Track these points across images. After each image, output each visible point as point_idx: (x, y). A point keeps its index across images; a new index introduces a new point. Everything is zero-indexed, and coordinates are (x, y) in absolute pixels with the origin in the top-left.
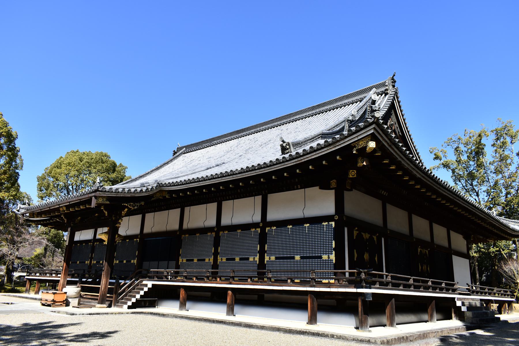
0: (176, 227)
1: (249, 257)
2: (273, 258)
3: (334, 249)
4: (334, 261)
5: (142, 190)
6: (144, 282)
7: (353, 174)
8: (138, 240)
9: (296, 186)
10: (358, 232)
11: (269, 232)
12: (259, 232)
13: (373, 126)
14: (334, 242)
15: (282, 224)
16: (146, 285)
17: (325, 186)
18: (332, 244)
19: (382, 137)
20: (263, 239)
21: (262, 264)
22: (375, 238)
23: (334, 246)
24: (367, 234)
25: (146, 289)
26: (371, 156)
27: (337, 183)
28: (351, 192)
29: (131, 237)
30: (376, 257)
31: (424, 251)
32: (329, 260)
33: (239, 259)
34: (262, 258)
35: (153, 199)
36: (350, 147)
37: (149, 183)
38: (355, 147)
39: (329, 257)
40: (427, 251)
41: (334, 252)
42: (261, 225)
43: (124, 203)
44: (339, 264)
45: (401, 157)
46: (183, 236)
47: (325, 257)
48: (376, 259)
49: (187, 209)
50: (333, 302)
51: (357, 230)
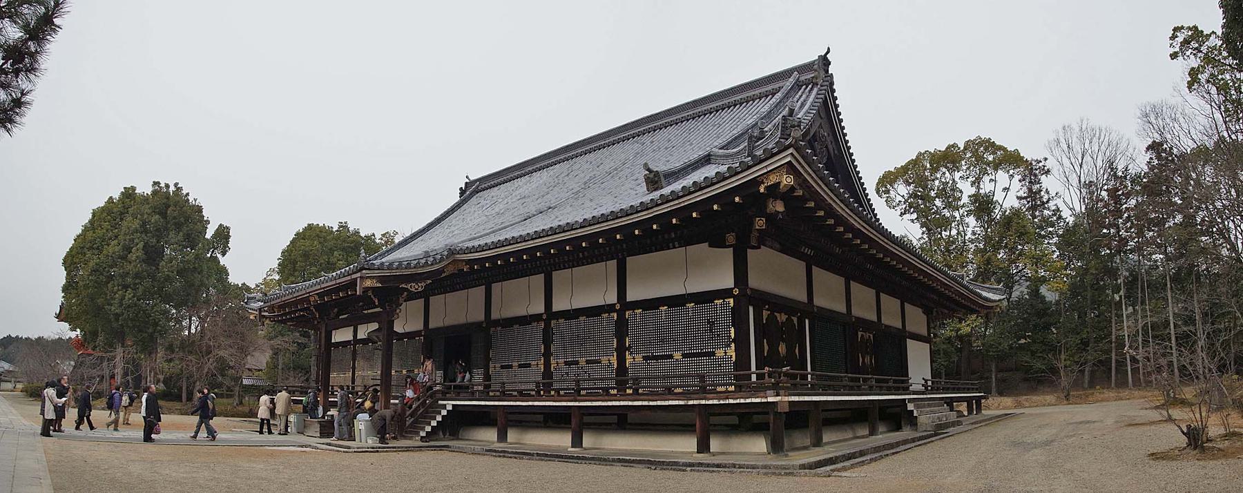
0: (481, 317)
2: (639, 358)
4: (734, 359)
5: (426, 262)
6: (440, 402)
7: (760, 223)
8: (422, 338)
9: (671, 244)
10: (769, 312)
12: (615, 318)
13: (791, 150)
14: (732, 330)
15: (650, 305)
16: (444, 407)
17: (717, 243)
18: (730, 333)
19: (803, 167)
20: (621, 329)
21: (622, 368)
22: (795, 320)
24: (783, 314)
25: (444, 412)
26: (787, 196)
27: (737, 238)
28: (759, 250)
29: (411, 335)
30: (797, 348)
31: (867, 335)
32: (726, 357)
34: (621, 360)
35: (443, 275)
36: (756, 182)
37: (436, 250)
38: (763, 183)
39: (726, 353)
40: (871, 335)
41: (733, 345)
42: (618, 307)
43: (402, 283)
44: (742, 362)
45: (831, 198)
46: (492, 329)
47: (720, 353)
48: (797, 351)
49: (496, 287)
50: (734, 420)
51: (767, 310)
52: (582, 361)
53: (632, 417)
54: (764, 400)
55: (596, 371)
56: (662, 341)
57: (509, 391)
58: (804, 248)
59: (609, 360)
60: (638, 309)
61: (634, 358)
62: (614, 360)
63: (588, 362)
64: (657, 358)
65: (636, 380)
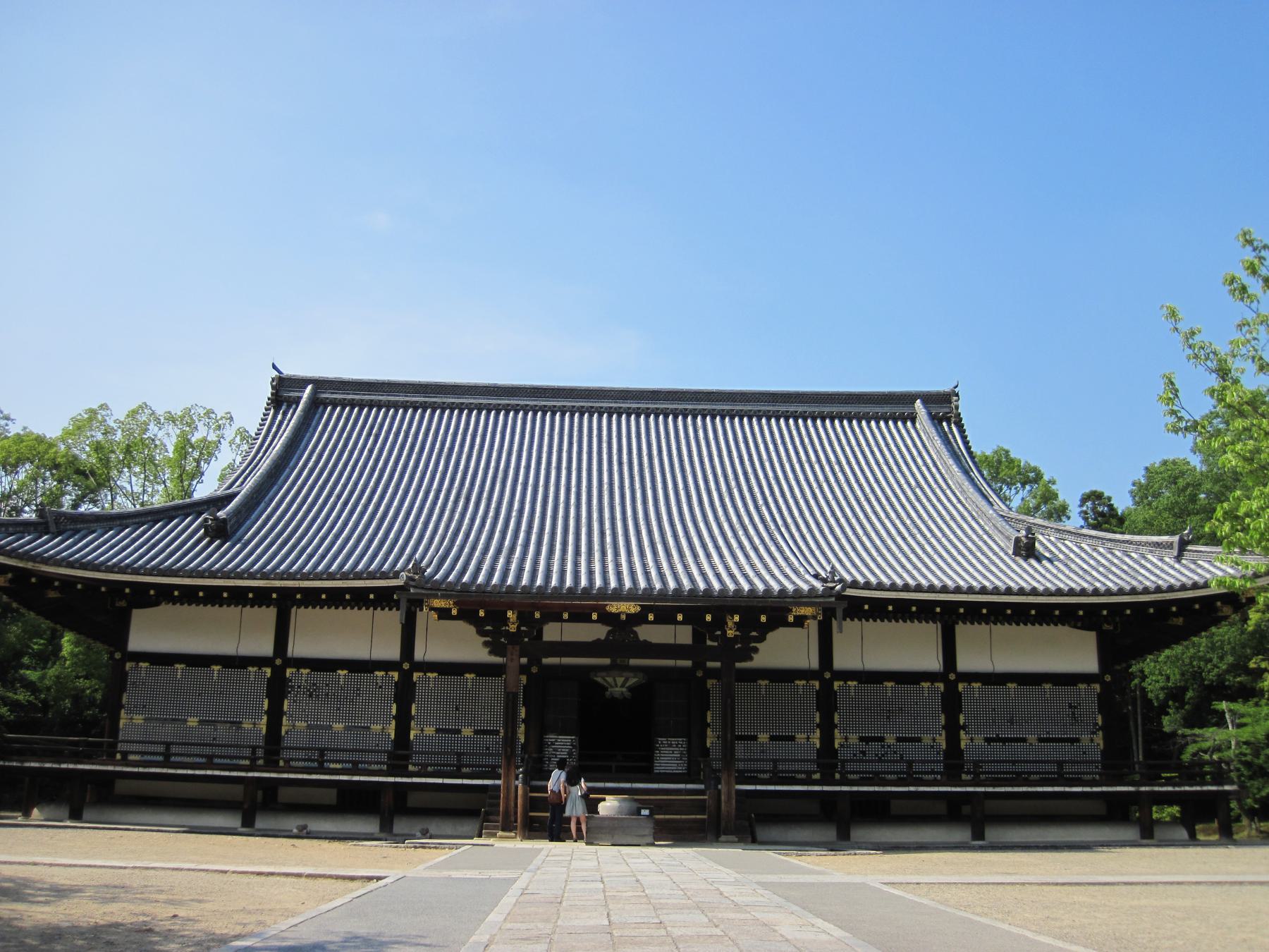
2: (979, 740)
3: (1101, 728)
4: (1102, 746)
20: (952, 704)
23: (1100, 723)
33: (769, 738)
34: (953, 739)
41: (1101, 733)
47: (1085, 738)
52: (890, 739)
54: (1220, 788)
55: (910, 750)
56: (1011, 722)
57: (922, 773)
58: (1217, 645)
59: (934, 740)
60: (976, 682)
61: (972, 740)
62: (942, 741)
63: (899, 740)
64: (1004, 740)
65: (976, 764)
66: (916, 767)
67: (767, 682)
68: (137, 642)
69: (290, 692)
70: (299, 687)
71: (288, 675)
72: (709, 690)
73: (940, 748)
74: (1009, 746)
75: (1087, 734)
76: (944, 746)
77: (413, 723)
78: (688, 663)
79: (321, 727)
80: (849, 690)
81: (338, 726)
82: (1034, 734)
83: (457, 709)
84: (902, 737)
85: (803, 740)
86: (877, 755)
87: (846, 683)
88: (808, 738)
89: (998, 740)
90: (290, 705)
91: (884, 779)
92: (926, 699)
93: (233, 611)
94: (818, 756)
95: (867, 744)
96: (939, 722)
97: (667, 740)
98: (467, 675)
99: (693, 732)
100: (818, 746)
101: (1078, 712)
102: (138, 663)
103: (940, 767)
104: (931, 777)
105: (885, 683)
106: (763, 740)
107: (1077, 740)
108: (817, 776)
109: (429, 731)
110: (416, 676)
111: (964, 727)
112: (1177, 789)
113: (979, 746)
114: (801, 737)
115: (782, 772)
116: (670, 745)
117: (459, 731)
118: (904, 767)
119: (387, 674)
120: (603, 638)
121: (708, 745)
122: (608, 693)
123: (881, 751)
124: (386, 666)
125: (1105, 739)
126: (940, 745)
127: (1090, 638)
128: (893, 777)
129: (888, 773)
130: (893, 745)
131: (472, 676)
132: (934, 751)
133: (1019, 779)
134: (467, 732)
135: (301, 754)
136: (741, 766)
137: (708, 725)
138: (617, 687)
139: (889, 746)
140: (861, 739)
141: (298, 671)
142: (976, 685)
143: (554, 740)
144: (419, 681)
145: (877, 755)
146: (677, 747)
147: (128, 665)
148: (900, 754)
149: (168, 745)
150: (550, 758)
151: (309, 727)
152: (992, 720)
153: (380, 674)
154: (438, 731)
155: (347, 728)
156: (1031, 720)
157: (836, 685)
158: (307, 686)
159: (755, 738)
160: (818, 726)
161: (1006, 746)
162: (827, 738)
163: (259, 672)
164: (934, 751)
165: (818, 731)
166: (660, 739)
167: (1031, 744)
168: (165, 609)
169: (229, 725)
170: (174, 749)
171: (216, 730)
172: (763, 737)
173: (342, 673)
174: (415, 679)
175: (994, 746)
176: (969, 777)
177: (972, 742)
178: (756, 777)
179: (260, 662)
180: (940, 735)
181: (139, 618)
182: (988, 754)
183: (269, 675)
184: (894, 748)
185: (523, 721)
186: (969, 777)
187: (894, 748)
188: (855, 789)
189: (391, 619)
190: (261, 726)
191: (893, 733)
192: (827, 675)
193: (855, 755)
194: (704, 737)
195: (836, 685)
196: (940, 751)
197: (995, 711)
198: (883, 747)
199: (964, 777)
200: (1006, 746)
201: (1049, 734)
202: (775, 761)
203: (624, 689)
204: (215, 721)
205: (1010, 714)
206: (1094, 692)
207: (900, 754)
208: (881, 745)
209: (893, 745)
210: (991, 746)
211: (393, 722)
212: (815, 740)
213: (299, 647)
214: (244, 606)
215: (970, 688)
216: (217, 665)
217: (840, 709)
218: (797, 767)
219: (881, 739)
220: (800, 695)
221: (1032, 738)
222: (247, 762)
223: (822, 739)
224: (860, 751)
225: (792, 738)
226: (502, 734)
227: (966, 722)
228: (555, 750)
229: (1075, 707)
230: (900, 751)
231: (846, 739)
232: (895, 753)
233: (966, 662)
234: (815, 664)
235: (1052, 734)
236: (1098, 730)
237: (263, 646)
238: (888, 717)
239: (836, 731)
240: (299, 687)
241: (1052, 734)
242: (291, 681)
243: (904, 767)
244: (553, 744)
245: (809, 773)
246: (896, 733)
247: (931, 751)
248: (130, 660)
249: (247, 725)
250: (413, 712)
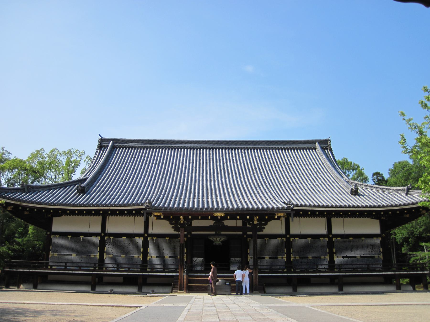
1: (265, 257)
2: (340, 257)
3: (382, 253)
4: (382, 259)
11: (282, 240)
20: (331, 245)
21: (332, 260)
23: (381, 251)
33: (269, 258)
34: (331, 257)
41: (382, 254)
47: (376, 256)
52: (310, 257)
53: (313, 281)
54: (423, 272)
55: (317, 261)
56: (351, 251)
59: (325, 257)
61: (338, 257)
63: (313, 257)
64: (349, 257)
65: (340, 265)
66: (319, 267)
67: (268, 239)
68: (55, 229)
69: (107, 245)
70: (110, 243)
71: (106, 239)
72: (248, 242)
73: (327, 260)
74: (350, 259)
75: (377, 255)
76: (328, 260)
77: (148, 255)
78: (241, 233)
79: (117, 256)
80: (296, 241)
81: (123, 256)
82: (359, 255)
83: (163, 250)
84: (314, 257)
85: (280, 258)
86: (305, 263)
87: (295, 239)
88: (282, 258)
89: (347, 257)
90: (107, 249)
91: (308, 271)
92: (322, 244)
93: (87, 218)
94: (285, 264)
95: (302, 259)
96: (326, 251)
97: (234, 259)
98: (166, 238)
99: (243, 256)
100: (286, 260)
101: (374, 247)
102: (55, 235)
103: (327, 267)
104: (324, 270)
105: (308, 238)
106: (267, 258)
107: (374, 257)
108: (285, 270)
109: (154, 257)
110: (149, 238)
111: (335, 253)
112: (408, 273)
113: (340, 259)
114: (280, 257)
115: (274, 269)
116: (235, 261)
117: (164, 257)
118: (315, 267)
119: (139, 238)
120: (212, 224)
121: (248, 260)
122: (214, 244)
123: (307, 262)
124: (139, 235)
125: (383, 256)
126: (327, 259)
127: (377, 222)
128: (311, 270)
129: (310, 269)
130: (311, 259)
131: (168, 238)
132: (325, 261)
133: (354, 270)
134: (167, 257)
135: (111, 266)
136: (259, 267)
137: (248, 254)
138: (217, 241)
139: (310, 260)
140: (300, 258)
141: (109, 237)
142: (339, 239)
143: (196, 260)
144: (150, 240)
145: (305, 263)
146: (238, 261)
147: (52, 236)
148: (314, 263)
149: (66, 263)
150: (195, 266)
151: (113, 256)
152: (345, 250)
153: (137, 238)
154: (157, 257)
155: (126, 257)
156: (358, 250)
157: (291, 239)
158: (112, 242)
159: (264, 258)
160: (285, 253)
161: (349, 259)
162: (289, 257)
163: (96, 238)
164: (325, 261)
165: (286, 255)
166: (232, 259)
167: (358, 258)
168: (64, 217)
169: (86, 256)
170: (68, 264)
171: (82, 258)
172: (267, 258)
173: (124, 238)
174: (149, 240)
175: (345, 259)
176: (337, 270)
177: (338, 258)
178: (265, 271)
179: (96, 234)
180: (327, 256)
181: (55, 220)
182: (343, 262)
183: (99, 239)
184: (311, 260)
185: (186, 253)
186: (337, 270)
187: (311, 260)
188: (299, 274)
189: (141, 220)
190: (97, 256)
191: (311, 255)
192: (288, 236)
193: (298, 263)
194: (247, 258)
195: (291, 239)
196: (327, 261)
197: (345, 247)
198: (308, 260)
199: (335, 270)
200: (349, 259)
201: (364, 255)
202: (271, 266)
203: (220, 242)
204: (81, 255)
205: (351, 248)
206: (379, 240)
207: (314, 263)
208: (307, 260)
209: (311, 259)
210: (344, 259)
211: (142, 254)
212: (285, 258)
213: (110, 229)
214: (91, 216)
215: (337, 240)
216: (82, 236)
217: (293, 248)
218: (279, 267)
219: (307, 257)
220: (279, 243)
221: (358, 256)
222: (93, 269)
223: (287, 258)
224: (300, 262)
225: (277, 258)
226: (179, 257)
227: (335, 251)
228: (197, 263)
229: (373, 246)
230: (313, 261)
231: (295, 257)
232: (312, 262)
233: (335, 231)
234: (284, 232)
235: (365, 255)
236: (381, 253)
237: (97, 229)
238: (309, 250)
239: (292, 255)
240: (110, 243)
241: (365, 255)
242: (107, 241)
243: (315, 267)
244: (196, 261)
245: (283, 269)
246: (312, 255)
247: (324, 261)
248: (53, 235)
249: (92, 256)
250: (148, 251)
